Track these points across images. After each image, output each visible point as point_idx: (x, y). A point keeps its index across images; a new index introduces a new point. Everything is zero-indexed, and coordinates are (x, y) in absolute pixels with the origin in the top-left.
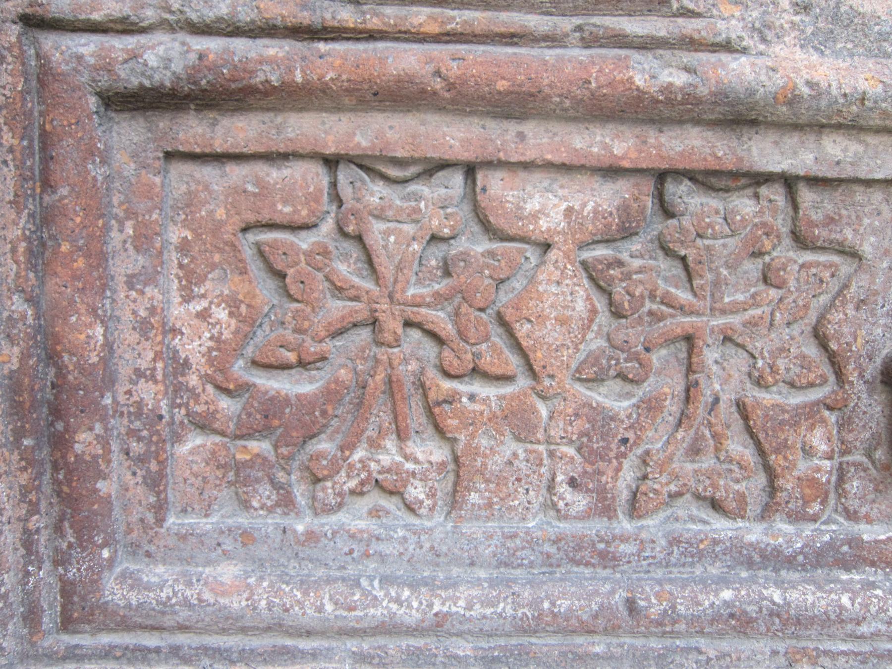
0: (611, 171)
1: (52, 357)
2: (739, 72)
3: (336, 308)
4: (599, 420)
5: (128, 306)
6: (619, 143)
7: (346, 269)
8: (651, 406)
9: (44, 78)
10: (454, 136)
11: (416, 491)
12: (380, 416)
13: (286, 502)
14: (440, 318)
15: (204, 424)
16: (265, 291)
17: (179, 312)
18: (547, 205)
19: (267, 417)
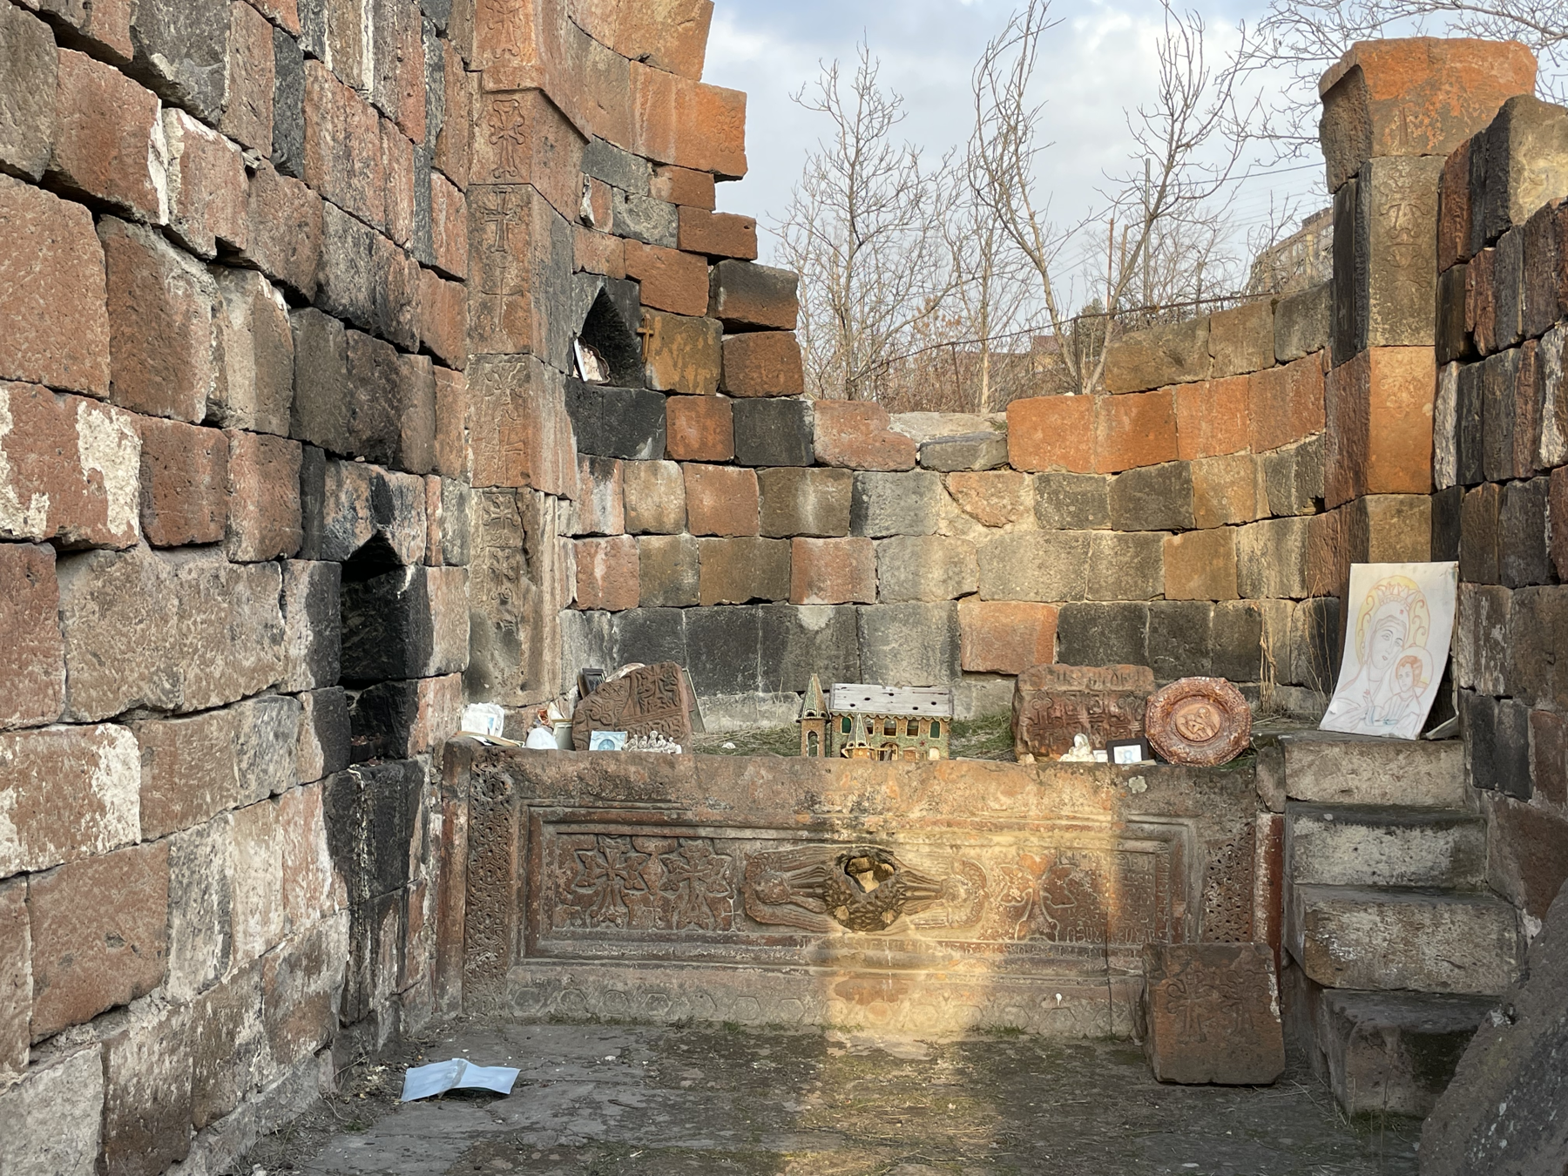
0: (665, 837)
1: (528, 884)
2: (689, 815)
3: (598, 871)
4: (666, 901)
5: (545, 870)
6: (667, 831)
7: (601, 861)
8: (680, 897)
9: (531, 818)
10: (626, 830)
11: (619, 921)
12: (609, 899)
13: (584, 925)
14: (624, 873)
15: (563, 902)
16: (580, 866)
17: (558, 872)
18: (652, 845)
19: (579, 899)
